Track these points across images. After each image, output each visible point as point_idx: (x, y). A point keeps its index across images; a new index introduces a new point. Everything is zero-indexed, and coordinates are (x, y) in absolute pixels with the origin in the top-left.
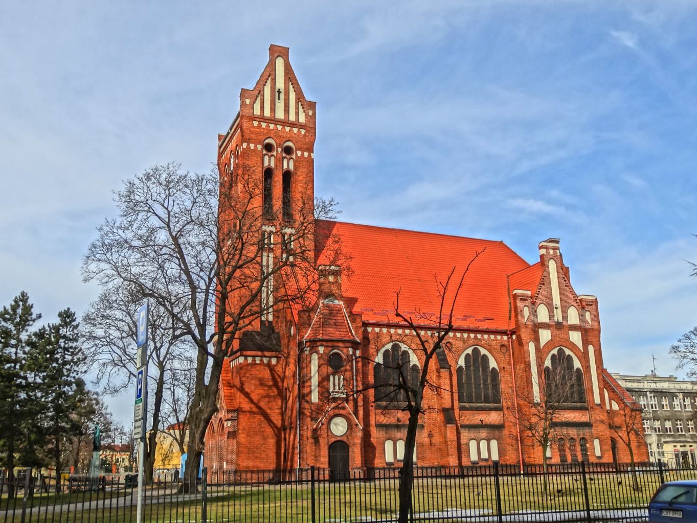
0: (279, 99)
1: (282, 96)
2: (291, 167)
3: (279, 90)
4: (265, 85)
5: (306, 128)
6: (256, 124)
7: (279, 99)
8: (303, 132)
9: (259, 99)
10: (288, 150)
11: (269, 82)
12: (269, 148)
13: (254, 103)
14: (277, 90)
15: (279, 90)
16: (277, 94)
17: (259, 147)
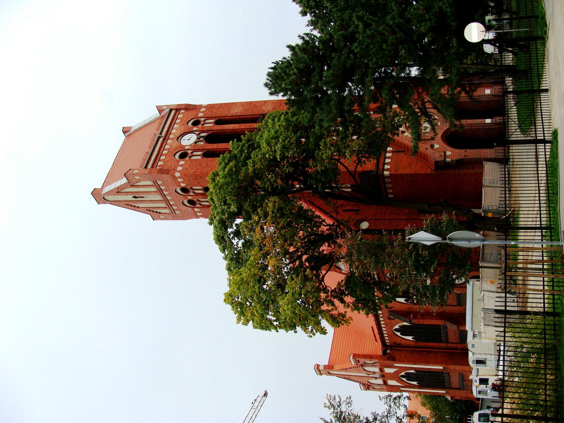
0: (143, 197)
1: (136, 196)
2: (200, 188)
3: (133, 197)
4: (138, 207)
5: (155, 181)
6: (177, 212)
7: (143, 197)
8: (159, 183)
9: (155, 210)
10: (184, 190)
11: (133, 205)
12: (191, 202)
13: (160, 213)
14: (134, 199)
15: (133, 197)
16: (138, 199)
17: (196, 210)
